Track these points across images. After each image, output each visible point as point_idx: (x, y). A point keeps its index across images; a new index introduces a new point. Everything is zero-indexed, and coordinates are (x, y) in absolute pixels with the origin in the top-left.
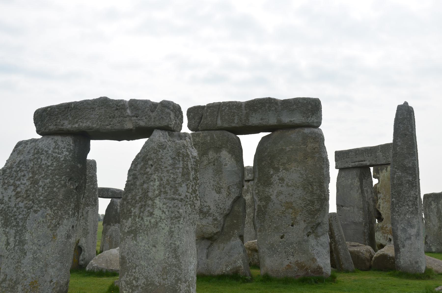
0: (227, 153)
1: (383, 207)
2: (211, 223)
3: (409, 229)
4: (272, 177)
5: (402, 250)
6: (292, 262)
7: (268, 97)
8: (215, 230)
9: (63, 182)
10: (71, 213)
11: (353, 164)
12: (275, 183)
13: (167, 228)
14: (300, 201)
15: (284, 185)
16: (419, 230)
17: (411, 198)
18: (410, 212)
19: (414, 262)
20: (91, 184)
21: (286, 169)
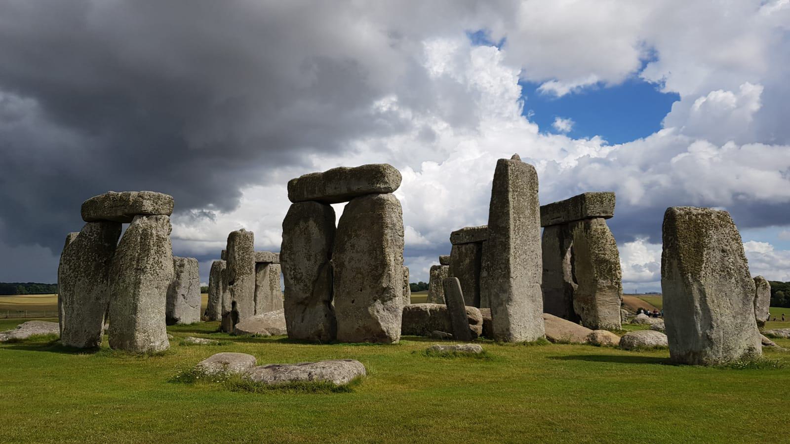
0: (313, 222)
1: (577, 271)
2: (302, 288)
3: (500, 294)
4: (345, 244)
5: (495, 316)
6: (361, 326)
7: (338, 167)
8: (304, 296)
9: (93, 258)
10: (99, 281)
11: (552, 221)
12: (347, 249)
13: (132, 291)
14: (367, 267)
15: (354, 251)
16: (510, 293)
17: (504, 261)
18: (502, 276)
19: (505, 330)
20: (247, 254)
21: (357, 236)
